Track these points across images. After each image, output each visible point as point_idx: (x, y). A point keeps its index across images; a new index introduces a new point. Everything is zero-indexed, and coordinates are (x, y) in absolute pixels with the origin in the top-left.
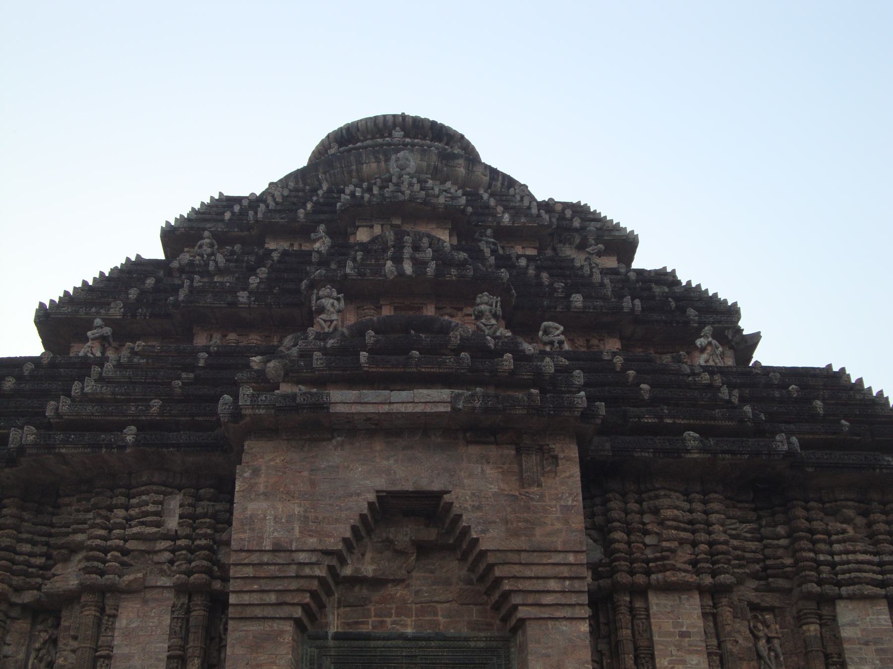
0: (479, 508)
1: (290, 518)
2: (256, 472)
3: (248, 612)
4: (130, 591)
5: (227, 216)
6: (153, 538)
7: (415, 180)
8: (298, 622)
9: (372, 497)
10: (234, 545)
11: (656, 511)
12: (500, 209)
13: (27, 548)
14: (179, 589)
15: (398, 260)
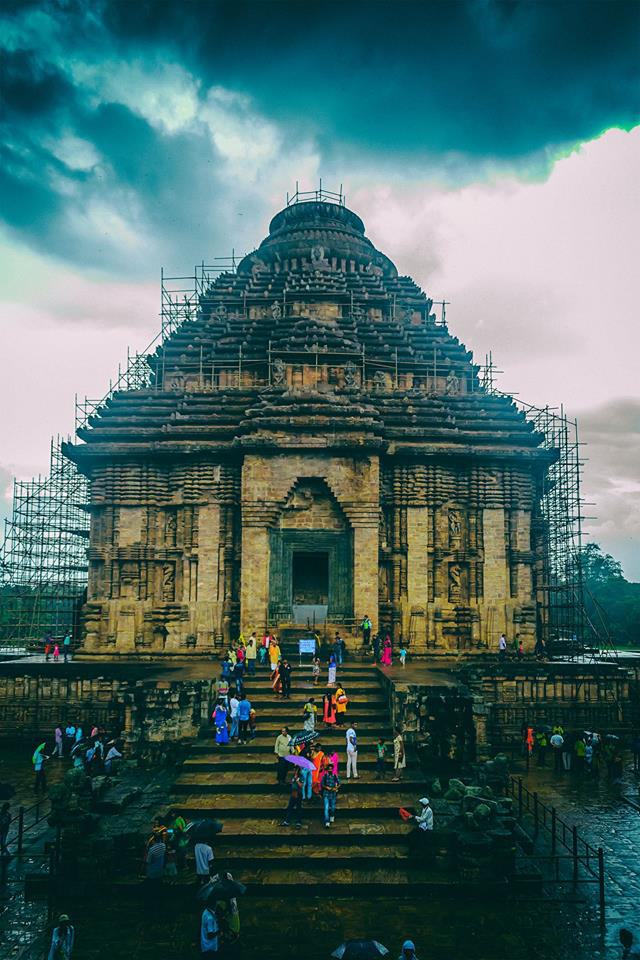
0: (338, 485)
1: (264, 489)
2: (249, 468)
3: (250, 524)
4: (204, 504)
5: (230, 289)
6: (212, 484)
7: (321, 276)
8: (268, 527)
9: (296, 480)
10: (243, 499)
11: (413, 474)
12: (364, 289)
13: (161, 484)
14: (222, 505)
15: (310, 345)
